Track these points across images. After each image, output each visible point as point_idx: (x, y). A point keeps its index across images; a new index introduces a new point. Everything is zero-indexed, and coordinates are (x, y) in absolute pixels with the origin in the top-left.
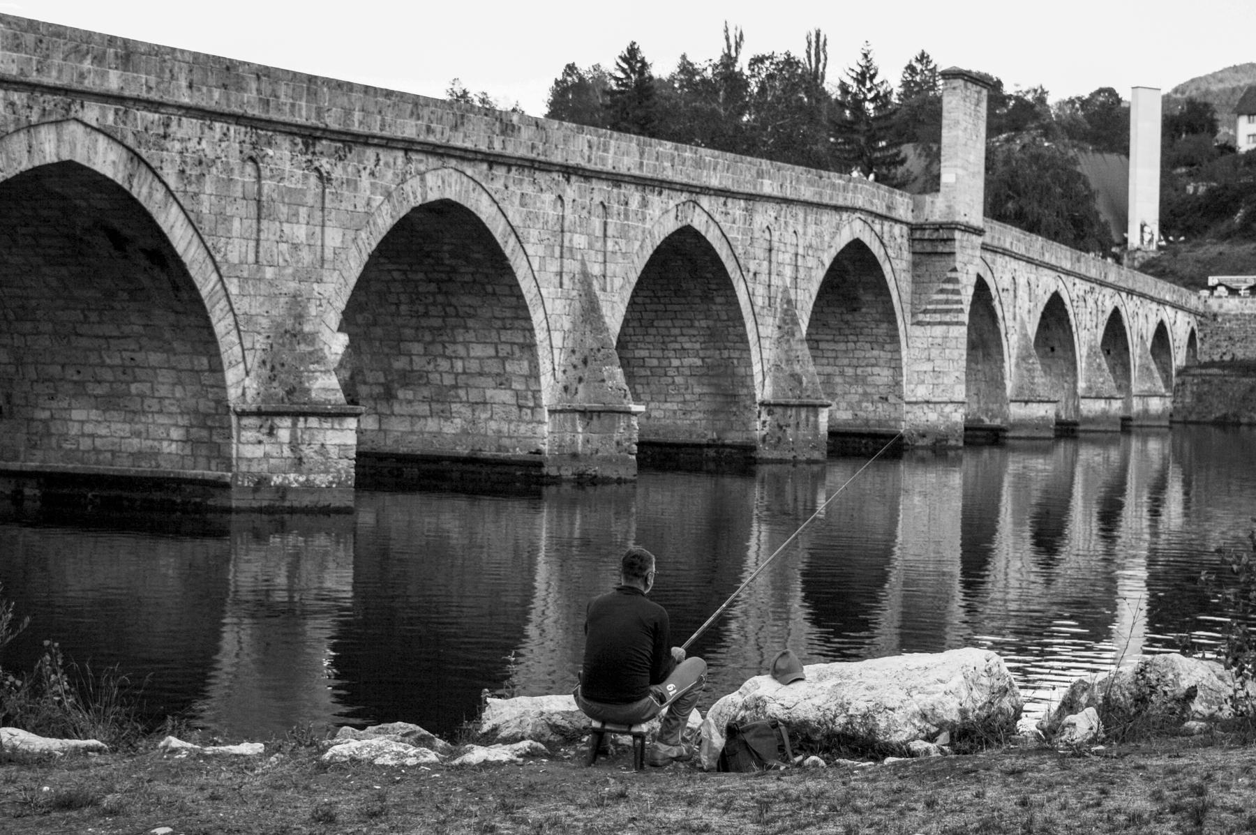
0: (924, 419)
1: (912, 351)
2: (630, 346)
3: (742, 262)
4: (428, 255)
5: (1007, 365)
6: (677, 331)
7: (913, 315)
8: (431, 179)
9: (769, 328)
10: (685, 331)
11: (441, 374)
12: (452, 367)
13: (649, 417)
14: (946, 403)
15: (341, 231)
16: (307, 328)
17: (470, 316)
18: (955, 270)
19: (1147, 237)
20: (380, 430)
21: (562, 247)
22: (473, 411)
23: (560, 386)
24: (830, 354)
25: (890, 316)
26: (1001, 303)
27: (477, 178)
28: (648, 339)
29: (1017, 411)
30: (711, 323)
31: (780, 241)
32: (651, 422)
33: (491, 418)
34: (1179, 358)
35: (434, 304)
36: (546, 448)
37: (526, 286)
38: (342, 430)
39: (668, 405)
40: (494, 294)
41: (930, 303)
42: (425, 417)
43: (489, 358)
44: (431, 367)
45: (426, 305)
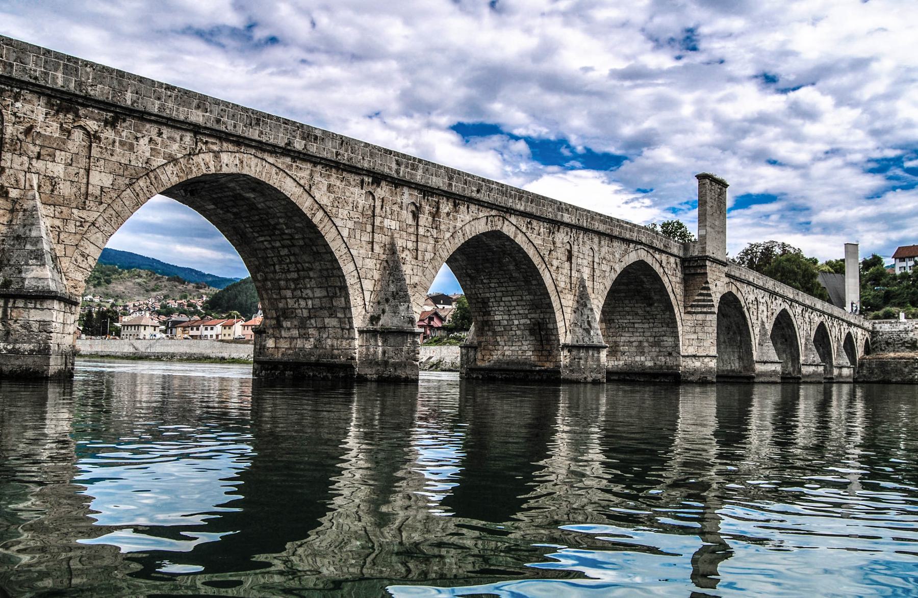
0: (693, 365)
1: (685, 328)
2: (492, 313)
3: (546, 259)
4: (275, 229)
5: (753, 343)
6: (514, 303)
7: (685, 307)
8: (225, 157)
9: (569, 301)
10: (519, 303)
11: (301, 309)
12: (307, 305)
13: (504, 355)
14: (706, 357)
15: (111, 177)
16: (34, 234)
17: (311, 269)
18: (707, 282)
19: (854, 309)
20: (276, 347)
21: (373, 225)
22: (319, 333)
23: (369, 315)
24: (640, 330)
25: (669, 307)
26: (748, 309)
27: (280, 166)
28: (501, 309)
29: (759, 368)
30: (532, 297)
31: (579, 251)
32: (505, 358)
33: (328, 337)
34: (860, 353)
35: (291, 263)
36: (357, 356)
37: (336, 246)
38: (43, 309)
39: (513, 348)
40: (318, 253)
41: (694, 301)
42: (296, 338)
43: (324, 297)
44: (296, 306)
45: (287, 264)
